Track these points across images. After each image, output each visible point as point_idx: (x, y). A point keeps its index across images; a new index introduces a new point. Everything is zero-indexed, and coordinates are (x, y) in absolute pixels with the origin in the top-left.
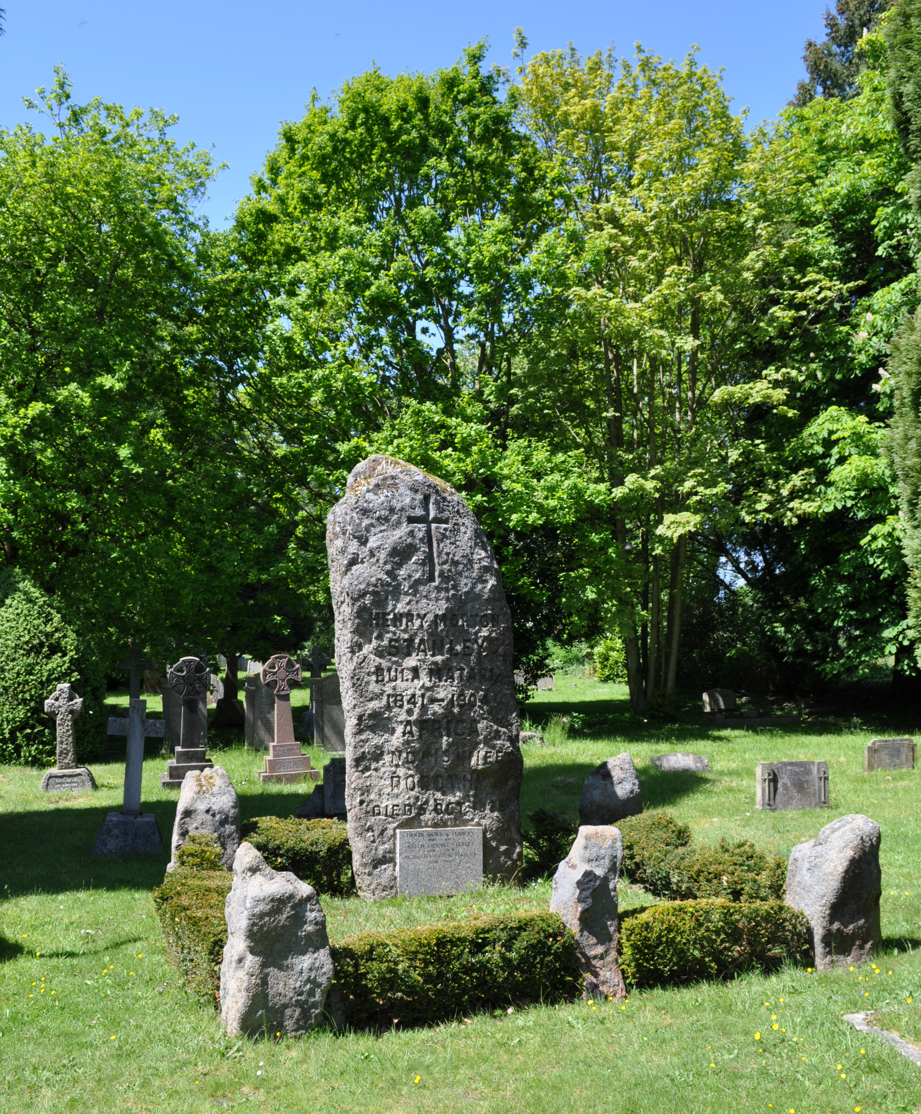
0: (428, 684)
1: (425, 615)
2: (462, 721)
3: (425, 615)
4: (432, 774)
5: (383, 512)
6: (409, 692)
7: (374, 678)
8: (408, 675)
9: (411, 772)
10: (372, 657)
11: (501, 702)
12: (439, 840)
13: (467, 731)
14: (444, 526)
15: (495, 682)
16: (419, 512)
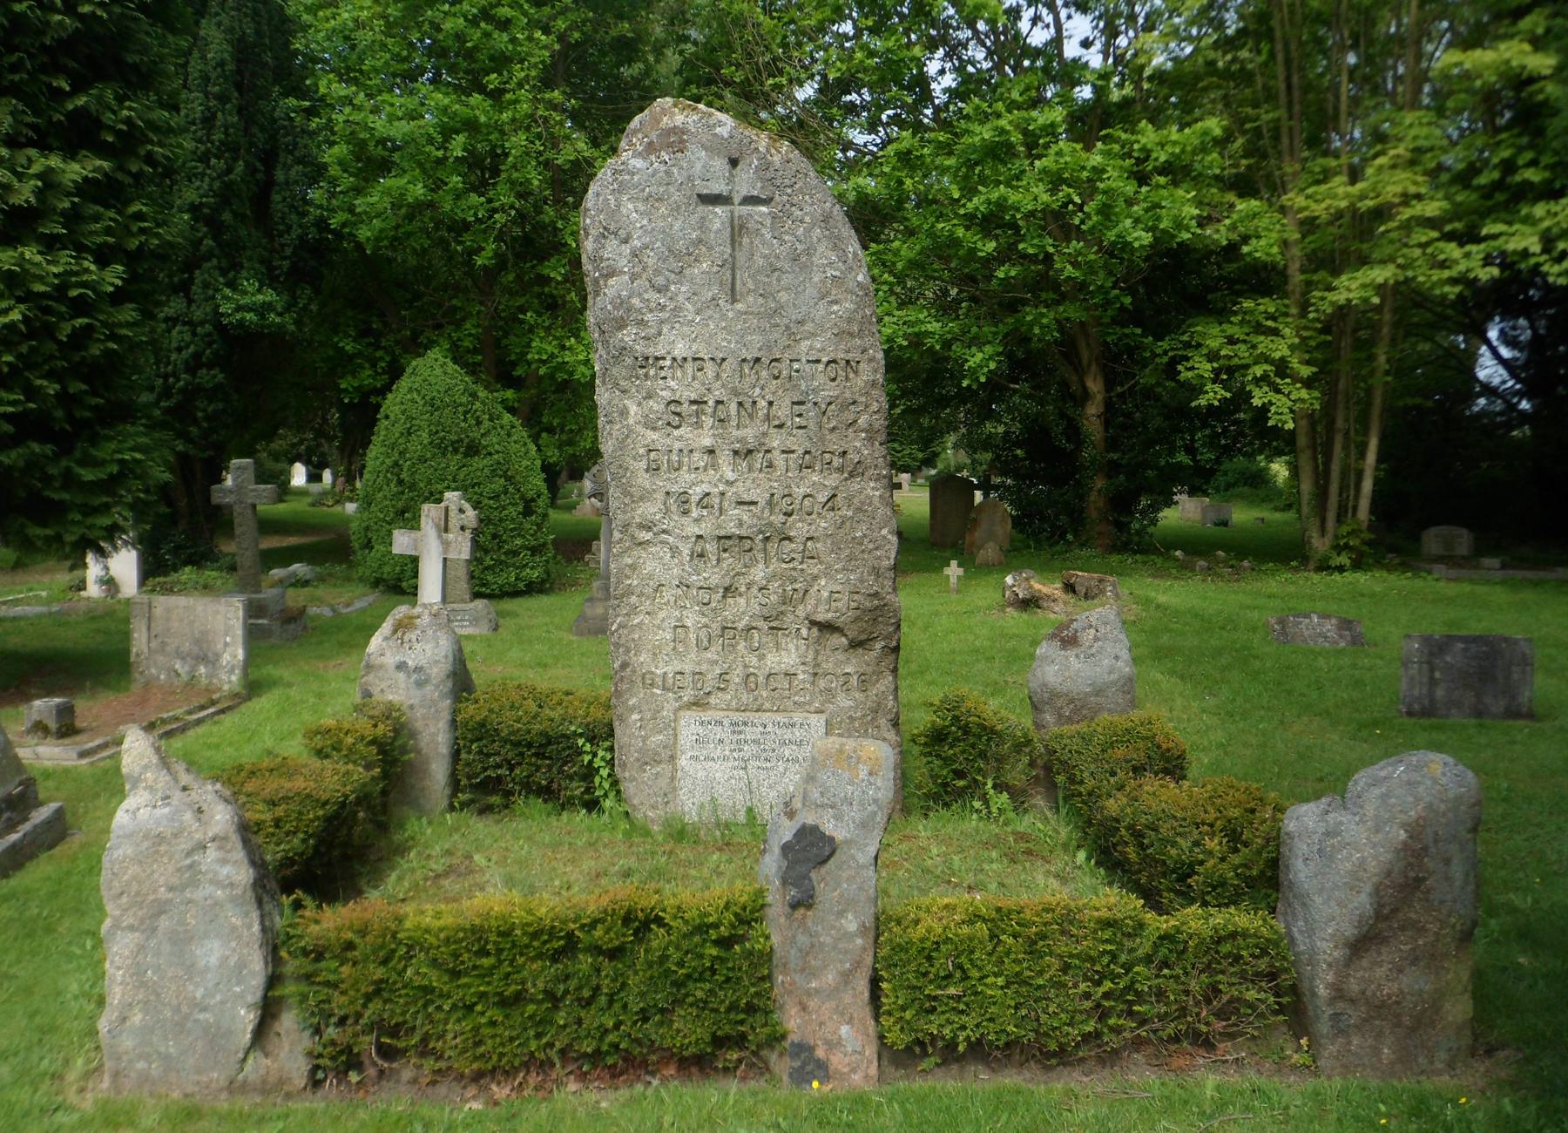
0: (730, 476)
1: (724, 360)
2: (789, 539)
3: (724, 360)
4: (741, 625)
5: (653, 189)
6: (698, 491)
7: (643, 464)
8: (700, 460)
9: (705, 620)
10: (639, 428)
11: (859, 510)
12: (750, 733)
13: (798, 557)
14: (764, 209)
15: (851, 475)
16: (718, 187)
